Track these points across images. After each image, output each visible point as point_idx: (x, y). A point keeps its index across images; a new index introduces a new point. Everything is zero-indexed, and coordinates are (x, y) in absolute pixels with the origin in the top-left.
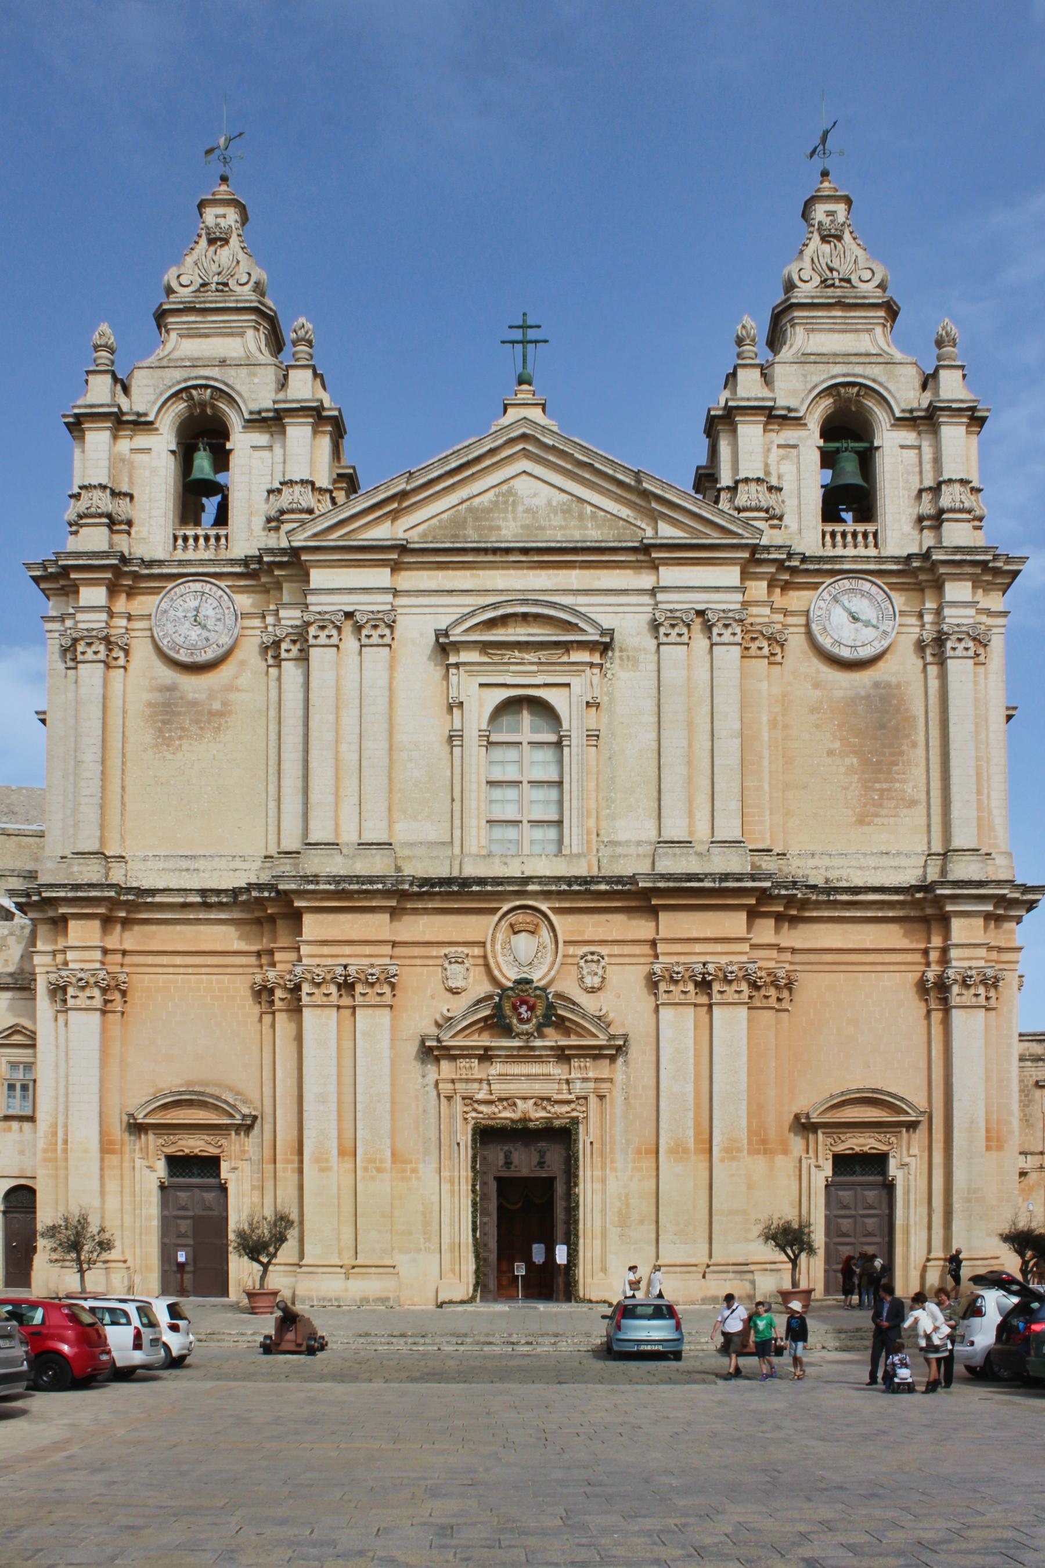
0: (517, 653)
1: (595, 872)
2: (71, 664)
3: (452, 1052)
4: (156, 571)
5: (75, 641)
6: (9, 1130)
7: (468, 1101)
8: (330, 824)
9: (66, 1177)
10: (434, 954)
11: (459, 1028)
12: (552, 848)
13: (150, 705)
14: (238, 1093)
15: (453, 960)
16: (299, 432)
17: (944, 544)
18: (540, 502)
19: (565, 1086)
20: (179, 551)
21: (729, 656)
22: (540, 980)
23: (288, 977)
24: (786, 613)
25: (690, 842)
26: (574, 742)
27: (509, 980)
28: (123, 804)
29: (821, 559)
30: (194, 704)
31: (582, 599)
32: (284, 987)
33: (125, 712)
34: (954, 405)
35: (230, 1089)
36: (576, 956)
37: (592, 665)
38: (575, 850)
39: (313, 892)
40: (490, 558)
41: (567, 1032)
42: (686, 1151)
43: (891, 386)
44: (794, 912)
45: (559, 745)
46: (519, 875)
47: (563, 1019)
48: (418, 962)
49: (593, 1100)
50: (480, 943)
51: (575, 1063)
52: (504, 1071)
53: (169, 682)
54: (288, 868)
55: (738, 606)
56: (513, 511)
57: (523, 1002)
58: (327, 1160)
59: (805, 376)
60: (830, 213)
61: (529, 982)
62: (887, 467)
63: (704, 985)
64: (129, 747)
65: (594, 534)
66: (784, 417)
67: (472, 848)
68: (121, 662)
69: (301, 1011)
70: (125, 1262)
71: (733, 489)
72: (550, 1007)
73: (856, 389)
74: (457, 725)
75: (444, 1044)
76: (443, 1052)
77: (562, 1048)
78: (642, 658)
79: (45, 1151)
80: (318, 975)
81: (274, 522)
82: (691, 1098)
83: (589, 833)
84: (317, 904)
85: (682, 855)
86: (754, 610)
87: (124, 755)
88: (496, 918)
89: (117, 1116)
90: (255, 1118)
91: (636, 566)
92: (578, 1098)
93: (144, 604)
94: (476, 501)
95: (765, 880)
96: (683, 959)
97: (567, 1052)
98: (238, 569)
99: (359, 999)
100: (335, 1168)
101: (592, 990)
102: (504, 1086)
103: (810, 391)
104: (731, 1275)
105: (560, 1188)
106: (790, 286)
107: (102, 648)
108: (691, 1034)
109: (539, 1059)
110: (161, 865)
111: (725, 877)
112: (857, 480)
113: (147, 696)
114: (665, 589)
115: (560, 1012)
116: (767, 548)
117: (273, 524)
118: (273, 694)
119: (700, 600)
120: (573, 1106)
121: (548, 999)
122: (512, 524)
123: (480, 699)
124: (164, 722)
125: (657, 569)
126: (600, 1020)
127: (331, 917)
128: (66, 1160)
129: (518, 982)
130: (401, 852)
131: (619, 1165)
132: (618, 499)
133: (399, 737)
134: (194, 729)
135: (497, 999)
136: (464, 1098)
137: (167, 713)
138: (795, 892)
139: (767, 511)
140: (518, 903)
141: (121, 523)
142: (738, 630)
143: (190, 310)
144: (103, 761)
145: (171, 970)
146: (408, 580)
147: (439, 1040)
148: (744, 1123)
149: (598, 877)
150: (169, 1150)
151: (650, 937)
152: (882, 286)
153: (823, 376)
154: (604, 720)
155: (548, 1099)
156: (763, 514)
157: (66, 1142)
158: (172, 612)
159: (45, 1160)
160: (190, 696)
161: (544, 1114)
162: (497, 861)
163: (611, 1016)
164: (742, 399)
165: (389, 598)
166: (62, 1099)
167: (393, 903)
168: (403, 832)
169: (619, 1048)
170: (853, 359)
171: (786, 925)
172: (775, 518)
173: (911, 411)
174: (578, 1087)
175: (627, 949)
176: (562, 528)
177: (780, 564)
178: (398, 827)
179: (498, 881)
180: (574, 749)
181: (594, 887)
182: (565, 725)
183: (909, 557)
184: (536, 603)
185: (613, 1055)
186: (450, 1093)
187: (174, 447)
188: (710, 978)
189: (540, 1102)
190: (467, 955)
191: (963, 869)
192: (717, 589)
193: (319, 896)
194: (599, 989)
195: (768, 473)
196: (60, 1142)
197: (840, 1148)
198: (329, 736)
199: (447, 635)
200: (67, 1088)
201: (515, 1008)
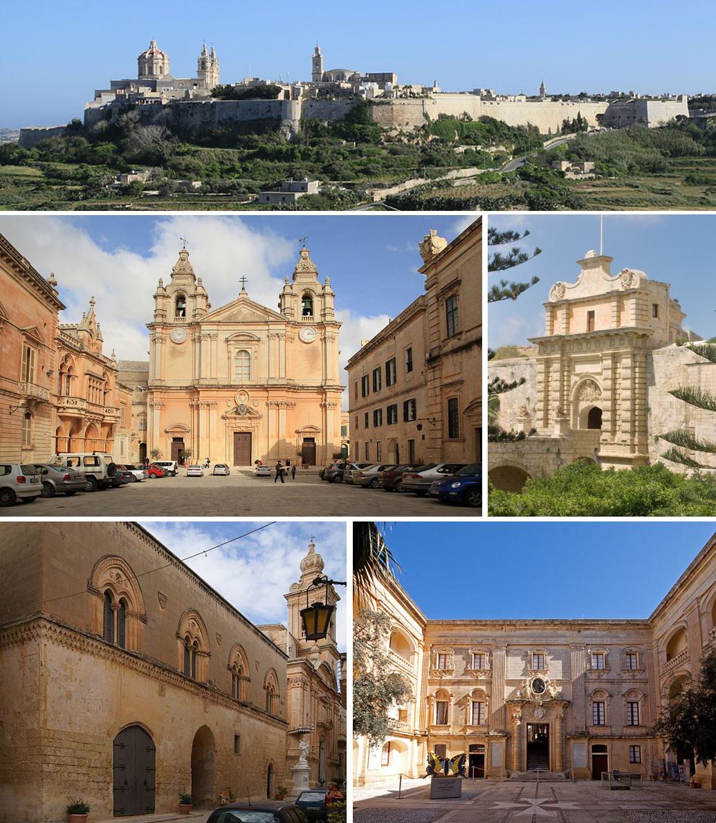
12: (248, 379)
16: (199, 299)
21: (283, 342)
24: (295, 333)
45: (249, 359)
49: (256, 428)
63: (278, 405)
65: (257, 319)
67: (232, 378)
71: (284, 309)
81: (194, 316)
93: (168, 331)
106: (297, 269)
112: (309, 307)
119: (277, 332)
126: (257, 412)
143: (177, 274)
146: (219, 328)
152: (315, 269)
168: (219, 376)
172: (292, 315)
177: (293, 324)
179: (237, 385)
191: (329, 383)
197: (305, 437)
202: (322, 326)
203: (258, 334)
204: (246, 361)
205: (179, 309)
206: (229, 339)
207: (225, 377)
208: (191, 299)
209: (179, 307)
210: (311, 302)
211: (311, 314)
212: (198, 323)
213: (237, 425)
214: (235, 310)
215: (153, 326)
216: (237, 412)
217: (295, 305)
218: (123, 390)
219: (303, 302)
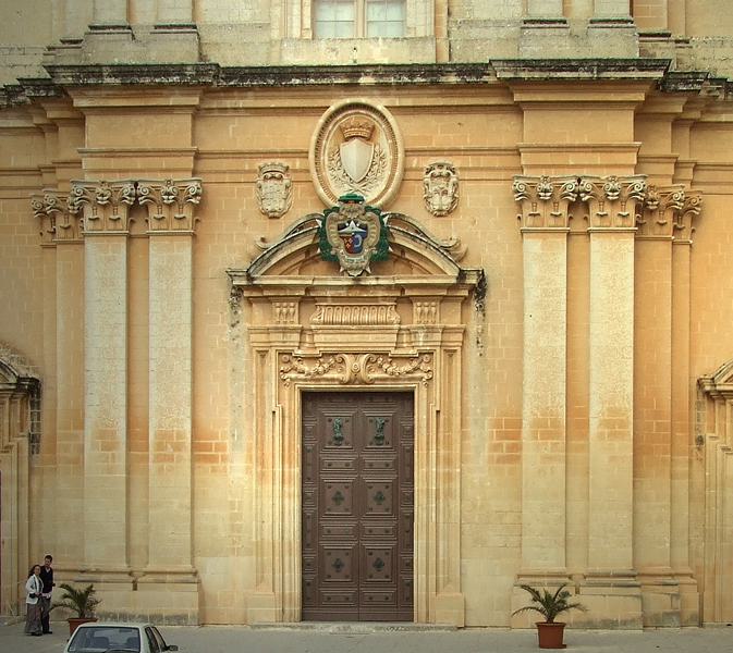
1: (445, 59)
3: (266, 293)
11: (274, 261)
15: (269, 175)
22: (376, 200)
23: (70, 199)
25: (565, 22)
36: (422, 170)
44: (695, 115)
46: (351, 63)
47: (403, 249)
48: (227, 178)
50: (302, 152)
51: (417, 308)
69: (83, 243)
75: (255, 282)
76: (255, 294)
77: (401, 288)
80: (102, 195)
82: (563, 355)
84: (102, 103)
88: (321, 120)
95: (655, 68)
96: (553, 174)
99: (153, 224)
101: (440, 214)
109: (373, 303)
111: (606, 64)
115: (398, 241)
120: (415, 364)
121: (382, 223)
127: (120, 120)
135: (320, 222)
138: (698, 87)
140: (348, 101)
147: (250, 278)
149: (445, 65)
151: (512, 145)
162: (323, 45)
163: (463, 250)
167: (195, 101)
169: (473, 289)
171: (687, 131)
175: (483, 161)
179: (323, 71)
181: (443, 79)
185: (466, 298)
188: (587, 197)
189: (375, 357)
190: (287, 168)
193: (104, 93)
194: (449, 212)
213: (324, 341)
216: (319, 252)
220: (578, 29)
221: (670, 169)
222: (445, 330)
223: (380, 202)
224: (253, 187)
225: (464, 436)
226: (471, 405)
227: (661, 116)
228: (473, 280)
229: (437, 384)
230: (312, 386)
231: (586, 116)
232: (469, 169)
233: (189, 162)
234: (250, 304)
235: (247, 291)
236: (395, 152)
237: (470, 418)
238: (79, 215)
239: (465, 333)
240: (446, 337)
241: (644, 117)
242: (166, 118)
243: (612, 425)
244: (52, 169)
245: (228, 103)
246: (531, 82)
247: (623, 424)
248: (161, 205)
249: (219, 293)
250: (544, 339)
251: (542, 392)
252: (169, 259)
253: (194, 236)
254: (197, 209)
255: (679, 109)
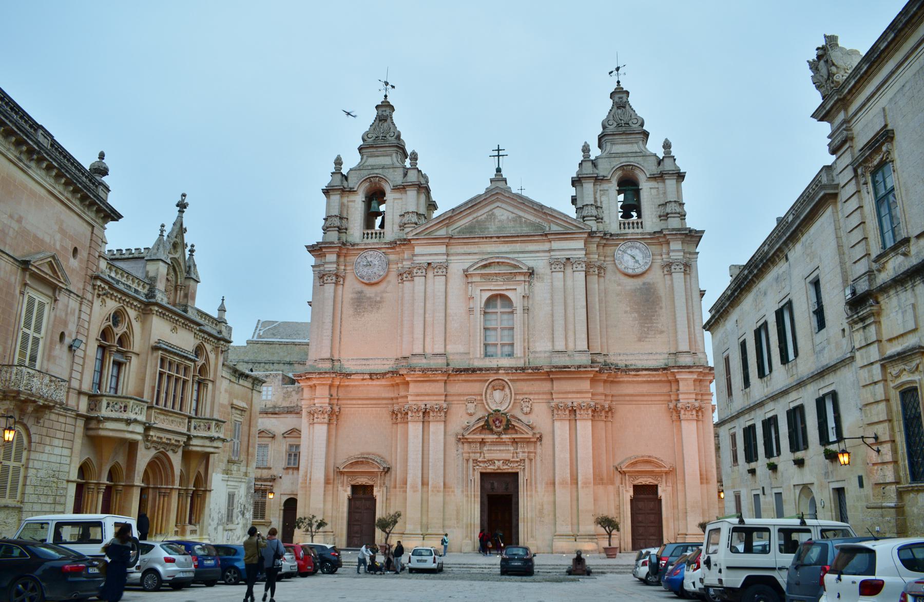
0: (495, 278)
1: (527, 365)
2: (322, 284)
3: (469, 440)
4: (356, 247)
5: (324, 275)
6: (288, 474)
7: (475, 461)
8: (421, 346)
9: (310, 495)
10: (462, 399)
11: (471, 430)
13: (352, 299)
14: (382, 458)
17: (669, 227)
18: (504, 218)
19: (515, 455)
20: (365, 239)
26: (518, 312)
27: (491, 409)
28: (340, 338)
29: (618, 235)
30: (370, 298)
31: (521, 255)
32: (401, 413)
33: (342, 302)
34: (670, 172)
35: (379, 456)
37: (525, 281)
38: (519, 356)
39: (414, 374)
40: (485, 240)
41: (516, 432)
42: (567, 483)
43: (645, 165)
45: (512, 313)
46: (495, 366)
48: (456, 402)
49: (527, 461)
51: (519, 445)
52: (490, 449)
53: (360, 290)
54: (404, 364)
55: (583, 256)
56: (494, 222)
57: (497, 419)
58: (417, 487)
59: (610, 163)
60: (620, 98)
61: (499, 411)
62: (645, 197)
63: (573, 411)
64: (344, 316)
66: (602, 180)
68: (341, 283)
70: (332, 532)
72: (508, 421)
73: (631, 167)
74: (472, 306)
77: (514, 439)
78: (545, 277)
79: (302, 483)
83: (524, 348)
85: (562, 357)
86: (592, 256)
87: (341, 319)
88: (487, 384)
89: (332, 468)
90: (389, 469)
91: (544, 241)
92: (521, 460)
94: (480, 218)
96: (563, 400)
97: (516, 440)
98: (387, 246)
99: (431, 418)
100: (420, 491)
101: (526, 414)
102: (490, 455)
103: (612, 169)
104: (587, 540)
105: (514, 500)
107: (334, 278)
108: (568, 432)
110: (354, 363)
113: (351, 296)
114: (553, 250)
116: (595, 232)
117: (402, 228)
118: (400, 294)
119: (568, 254)
120: (519, 463)
122: (493, 227)
123: (481, 295)
124: (358, 306)
125: (550, 242)
127: (421, 384)
128: (310, 487)
129: (495, 411)
130: (451, 357)
131: (539, 489)
132: (535, 216)
133: (449, 311)
134: (369, 308)
135: (486, 418)
136: (473, 460)
137: (359, 302)
139: (596, 217)
141: (343, 229)
142: (584, 265)
144: (333, 322)
145: (357, 406)
147: (463, 435)
148: (591, 471)
150: (353, 483)
153: (617, 163)
154: (531, 302)
155: (509, 460)
156: (594, 218)
157: (310, 479)
158: (362, 263)
159: (302, 487)
160: (368, 295)
161: (507, 467)
164: (584, 174)
165: (445, 257)
166: (310, 461)
168: (451, 348)
169: (538, 438)
170: (630, 155)
173: (654, 175)
174: (521, 456)
175: (540, 397)
176: (513, 227)
178: (448, 347)
179: (488, 369)
180: (518, 315)
182: (515, 305)
183: (655, 232)
184: (502, 258)
186: (467, 458)
187: (364, 199)
192: (575, 250)
195: (596, 201)
196: (308, 479)
198: (422, 312)
199: (467, 271)
200: (312, 456)
201: (494, 422)
202: (659, 238)
203: (529, 261)
204: (505, 317)
205: (370, 216)
206: (471, 271)
207: (462, 350)
208: (397, 195)
209: (372, 210)
210: (637, 192)
211: (639, 216)
212: (406, 242)
213: (488, 456)
214: (481, 214)
215: (321, 248)
216: (487, 427)
217: (604, 199)
218: (241, 382)
219: (619, 192)
220: (570, 353)
221: (603, 397)
222: (529, 452)
223: (506, 411)
224: (464, 405)
225: (536, 488)
226: (538, 477)
227: (599, 381)
228: (538, 436)
229: (526, 470)
230: (484, 471)
231: (574, 382)
232: (536, 399)
233: (443, 398)
234: (463, 443)
235: (462, 440)
236: (511, 394)
237: (538, 482)
238: (407, 413)
239: (535, 453)
240: (529, 454)
241: (593, 381)
242: (436, 384)
243: (586, 484)
244: (397, 398)
245: (456, 379)
246: (556, 372)
247: (590, 483)
248: (433, 411)
249: (452, 440)
250: (562, 455)
251: (563, 472)
252: (436, 429)
253: (445, 421)
254: (446, 413)
255: (606, 378)
